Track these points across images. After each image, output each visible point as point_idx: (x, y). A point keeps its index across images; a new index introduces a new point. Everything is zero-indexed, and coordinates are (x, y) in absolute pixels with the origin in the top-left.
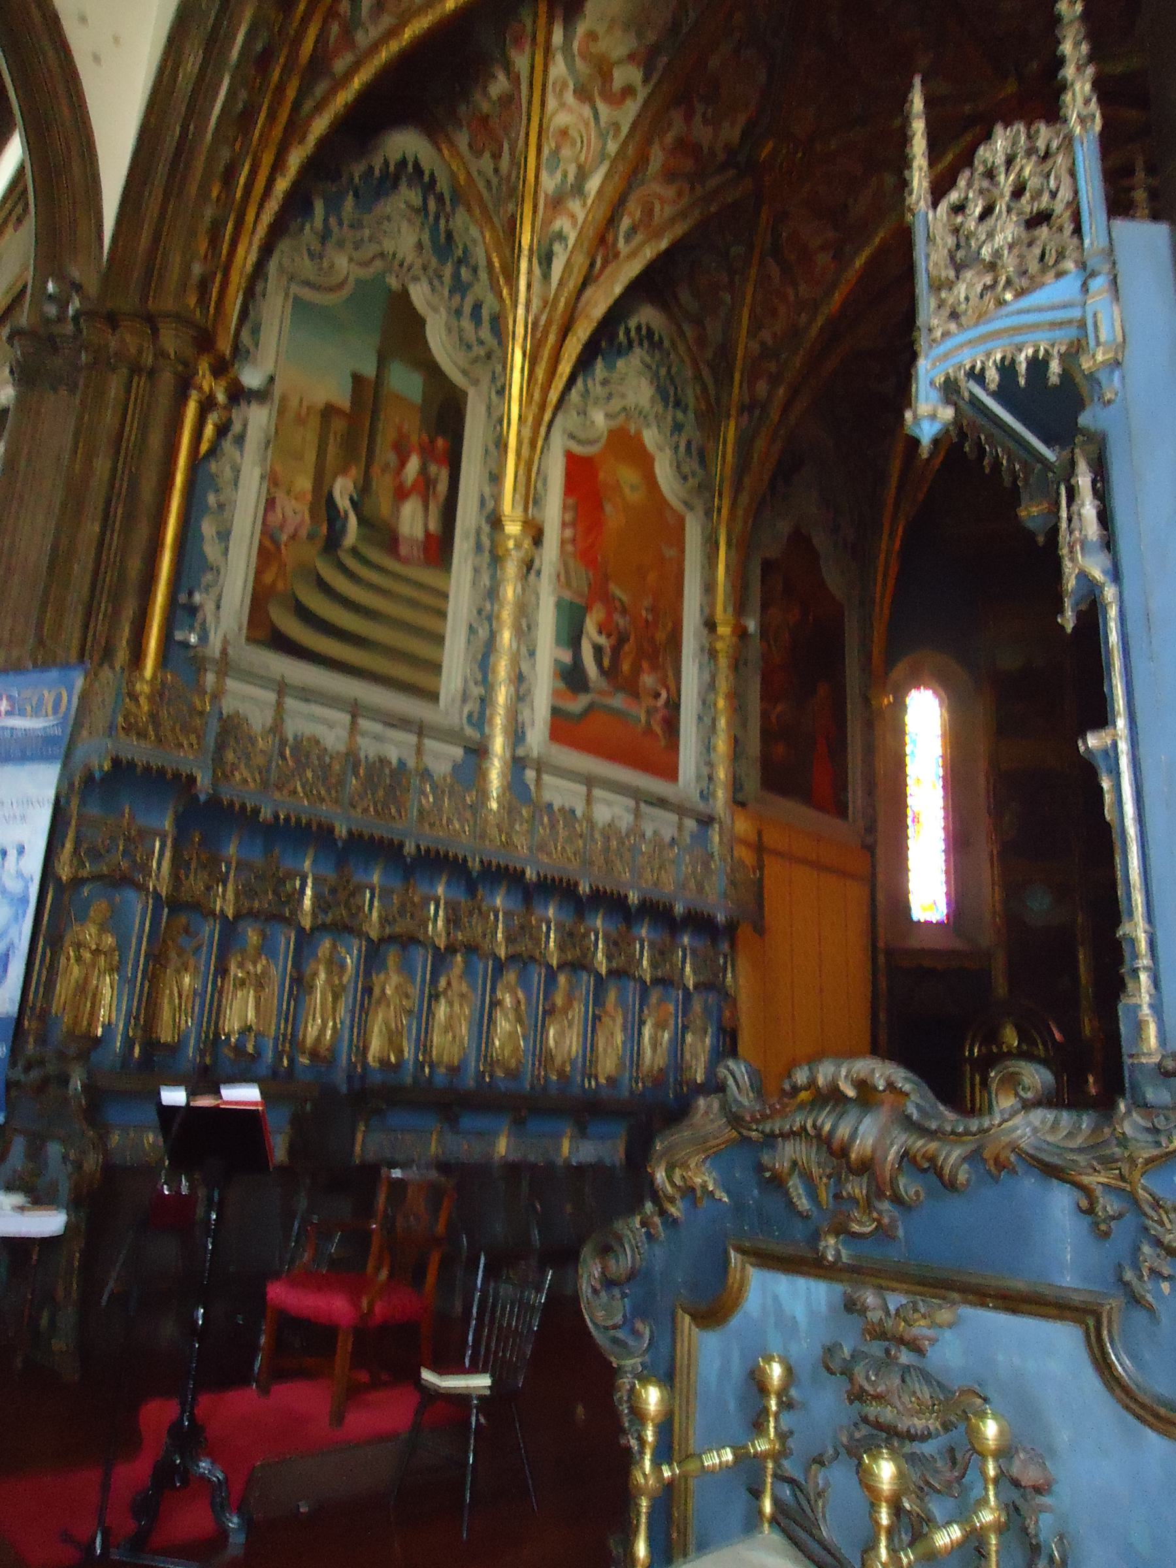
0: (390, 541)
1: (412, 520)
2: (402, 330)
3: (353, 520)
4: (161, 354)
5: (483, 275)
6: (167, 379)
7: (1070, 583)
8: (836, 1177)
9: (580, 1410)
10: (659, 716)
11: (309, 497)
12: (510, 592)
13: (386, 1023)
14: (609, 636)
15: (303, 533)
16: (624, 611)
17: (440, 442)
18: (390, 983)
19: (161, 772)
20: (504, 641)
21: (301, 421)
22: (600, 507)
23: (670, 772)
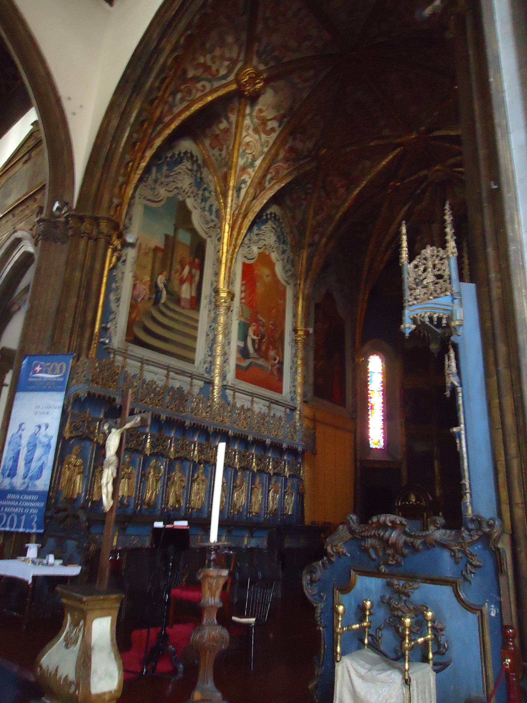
1: (186, 292)
2: (183, 217)
3: (164, 293)
4: (100, 233)
5: (213, 194)
7: (449, 385)
8: (384, 549)
9: (271, 635)
10: (275, 367)
11: (149, 283)
12: (222, 319)
13: (175, 491)
14: (257, 336)
16: (263, 326)
17: (197, 260)
18: (177, 476)
19: (104, 397)
20: (219, 339)
21: (146, 254)
22: (254, 284)
23: (279, 390)
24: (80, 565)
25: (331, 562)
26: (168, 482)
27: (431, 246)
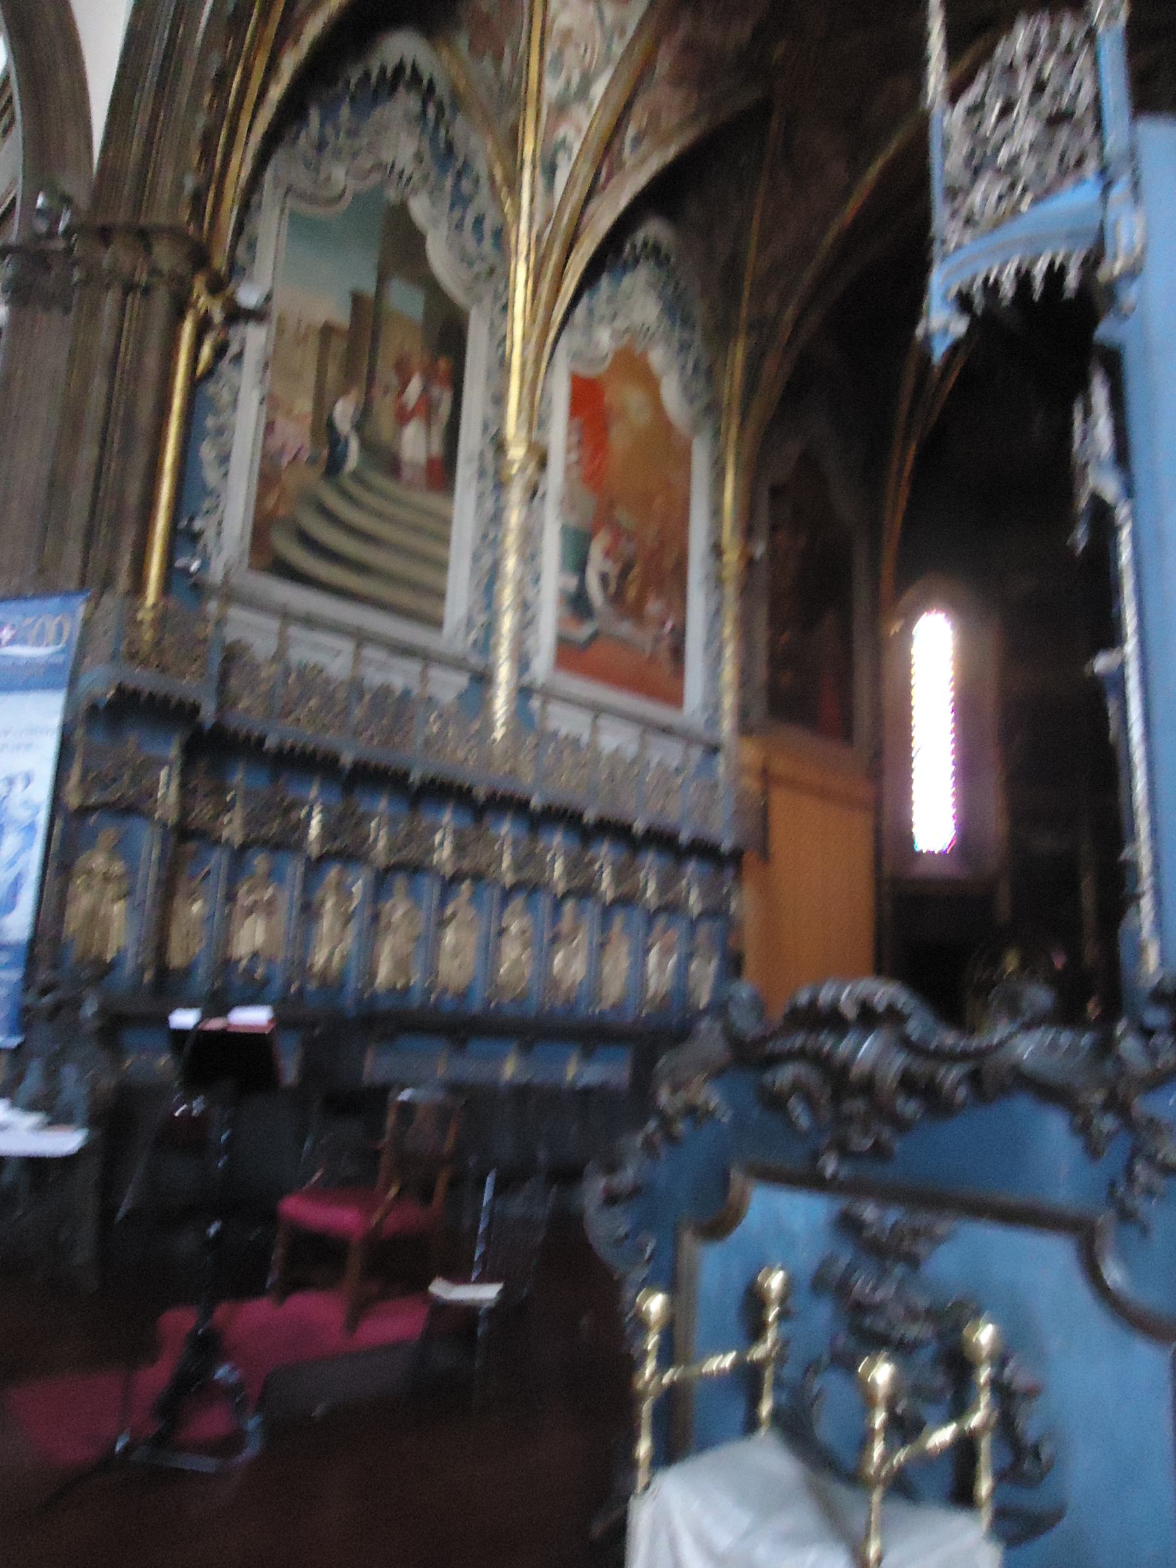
0: (393, 466)
1: (415, 444)
2: (403, 246)
3: (354, 445)
4: (154, 271)
5: (485, 190)
6: (161, 299)
7: (1083, 502)
8: (837, 1098)
12: (514, 517)
15: (305, 456)
18: (398, 909)
19: (166, 700)
21: (301, 340)
23: (675, 698)
24: (82, 1127)
25: (671, 1139)
26: (375, 924)
27: (1032, 12)
